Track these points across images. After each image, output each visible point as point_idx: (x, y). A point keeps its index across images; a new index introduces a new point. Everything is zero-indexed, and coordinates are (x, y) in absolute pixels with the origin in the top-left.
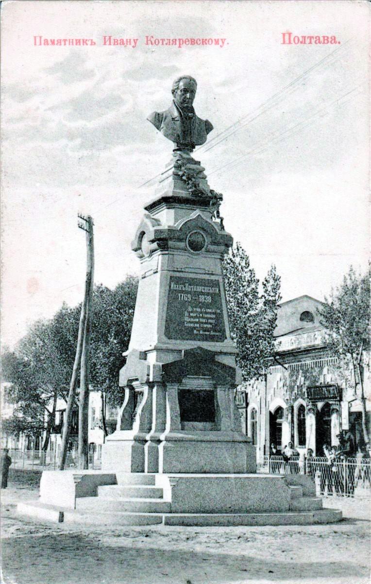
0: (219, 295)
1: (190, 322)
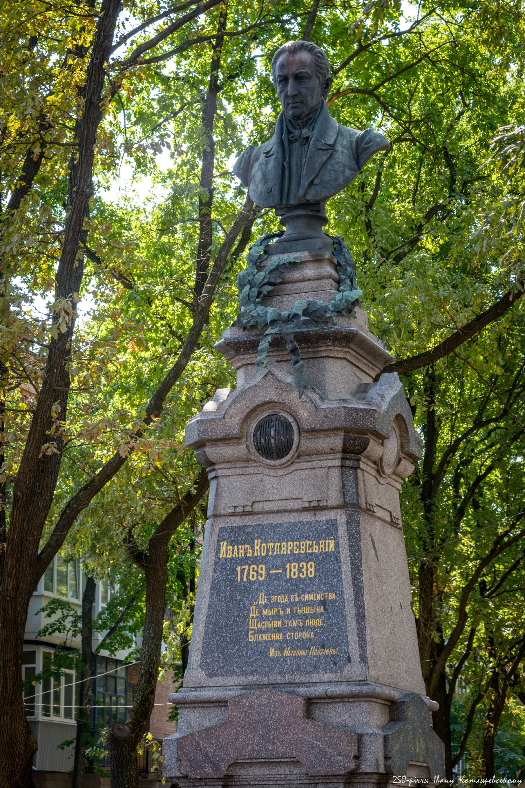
0: (336, 556)
1: (261, 631)
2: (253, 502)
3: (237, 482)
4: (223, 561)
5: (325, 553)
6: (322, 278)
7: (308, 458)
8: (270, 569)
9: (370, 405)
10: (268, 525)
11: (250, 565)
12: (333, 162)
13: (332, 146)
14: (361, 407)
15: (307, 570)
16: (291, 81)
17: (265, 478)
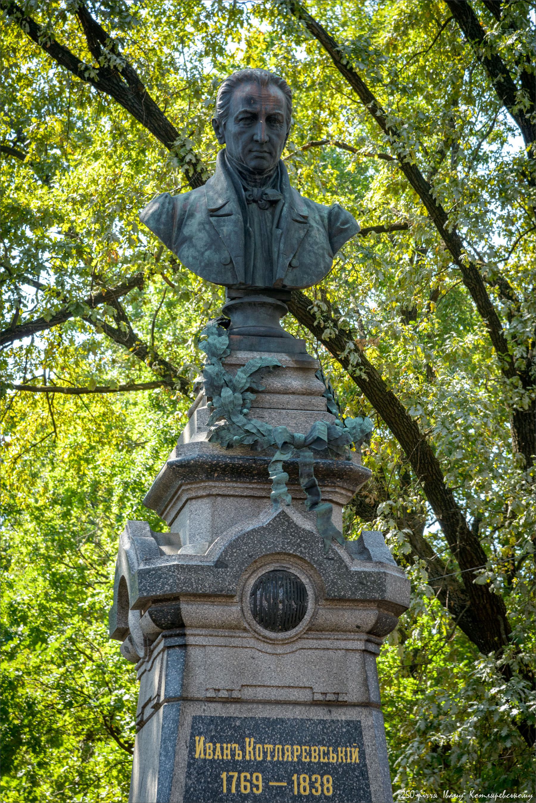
0: (361, 770)
2: (242, 686)
3: (218, 656)
4: (201, 763)
5: (346, 764)
7: (319, 635)
8: (269, 780)
10: (264, 719)
11: (240, 773)
15: (322, 785)
17: (257, 654)
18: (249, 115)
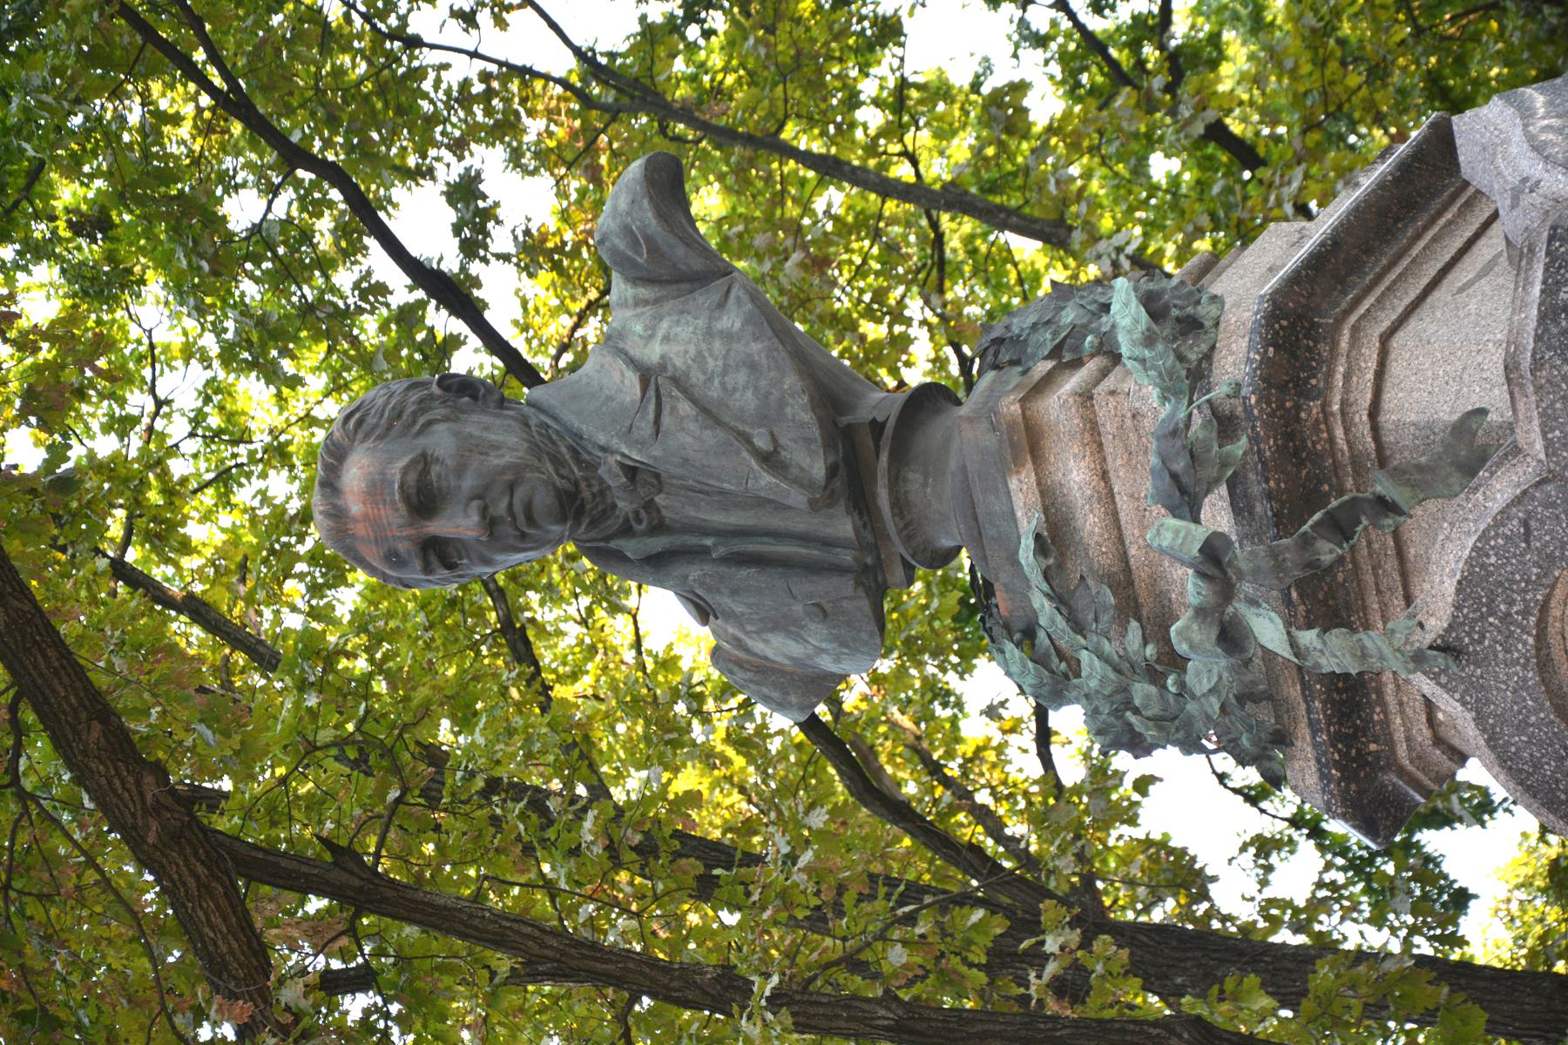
6: (1093, 427)
9: (1531, 250)
12: (696, 377)
13: (647, 375)
14: (1537, 289)
16: (439, 527)
18: (433, 559)
